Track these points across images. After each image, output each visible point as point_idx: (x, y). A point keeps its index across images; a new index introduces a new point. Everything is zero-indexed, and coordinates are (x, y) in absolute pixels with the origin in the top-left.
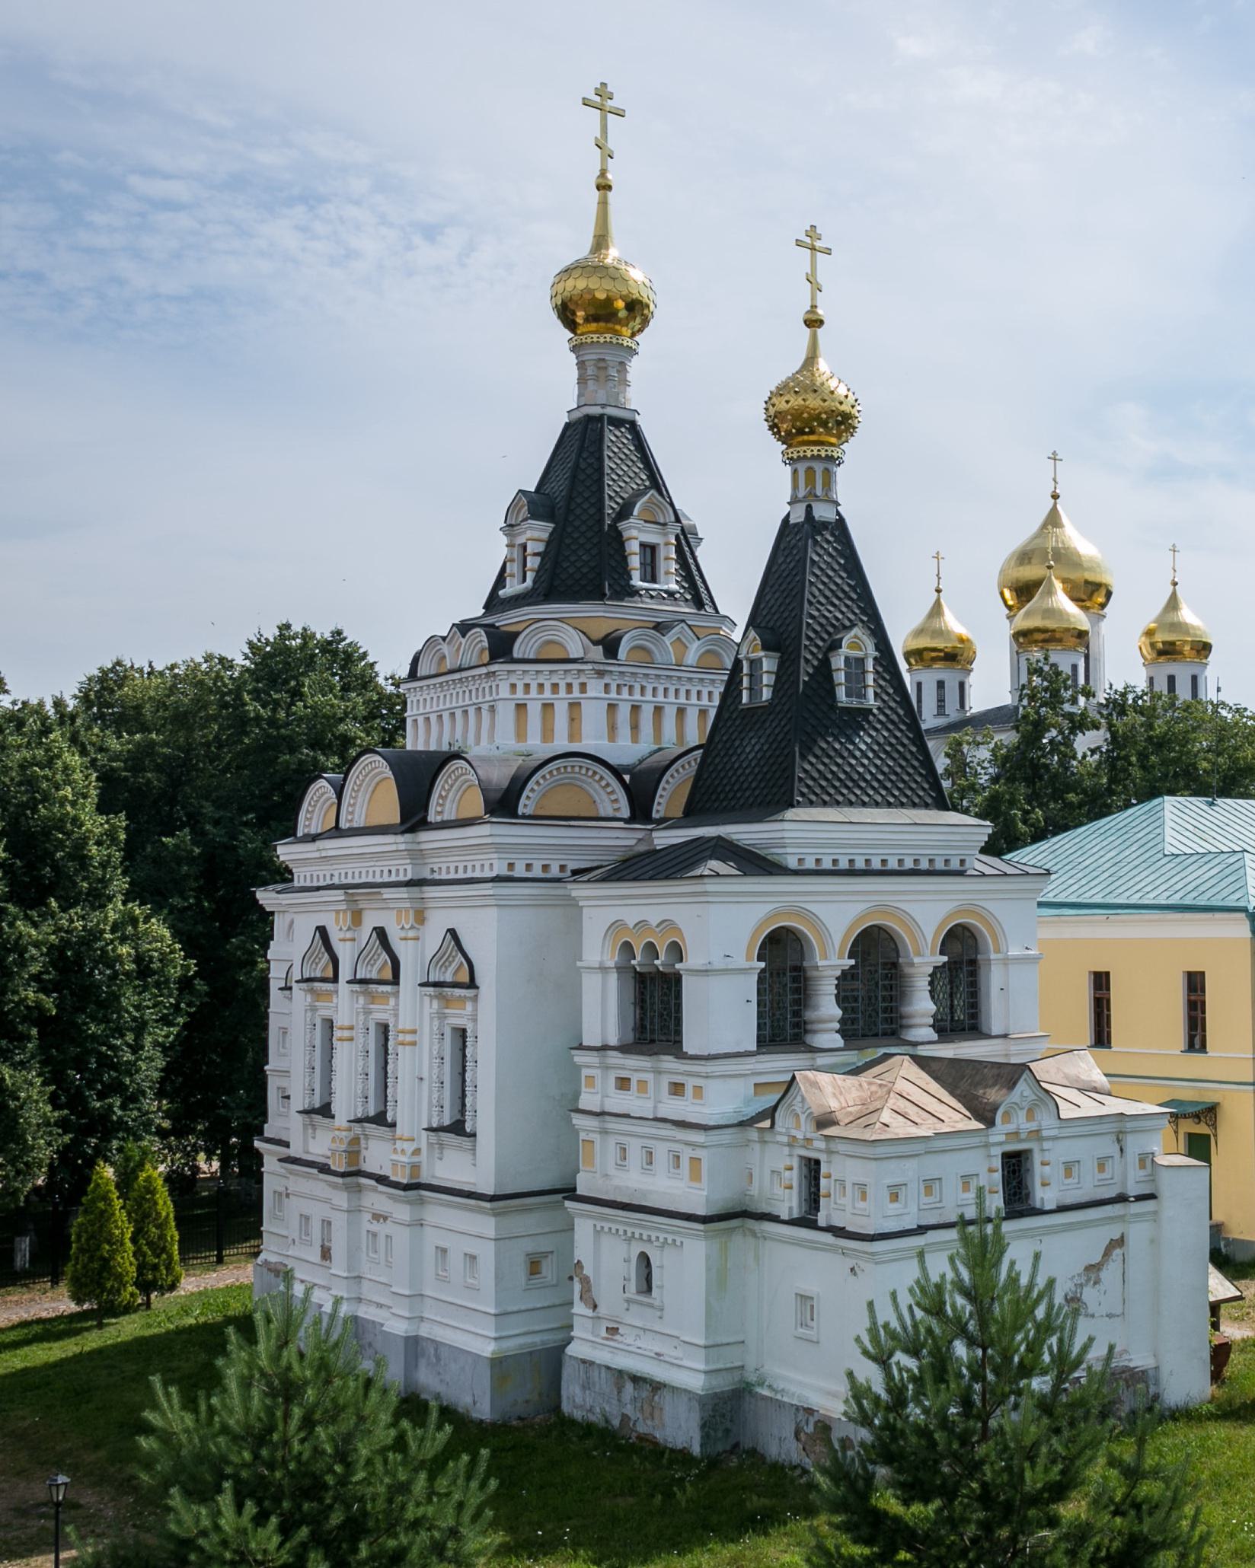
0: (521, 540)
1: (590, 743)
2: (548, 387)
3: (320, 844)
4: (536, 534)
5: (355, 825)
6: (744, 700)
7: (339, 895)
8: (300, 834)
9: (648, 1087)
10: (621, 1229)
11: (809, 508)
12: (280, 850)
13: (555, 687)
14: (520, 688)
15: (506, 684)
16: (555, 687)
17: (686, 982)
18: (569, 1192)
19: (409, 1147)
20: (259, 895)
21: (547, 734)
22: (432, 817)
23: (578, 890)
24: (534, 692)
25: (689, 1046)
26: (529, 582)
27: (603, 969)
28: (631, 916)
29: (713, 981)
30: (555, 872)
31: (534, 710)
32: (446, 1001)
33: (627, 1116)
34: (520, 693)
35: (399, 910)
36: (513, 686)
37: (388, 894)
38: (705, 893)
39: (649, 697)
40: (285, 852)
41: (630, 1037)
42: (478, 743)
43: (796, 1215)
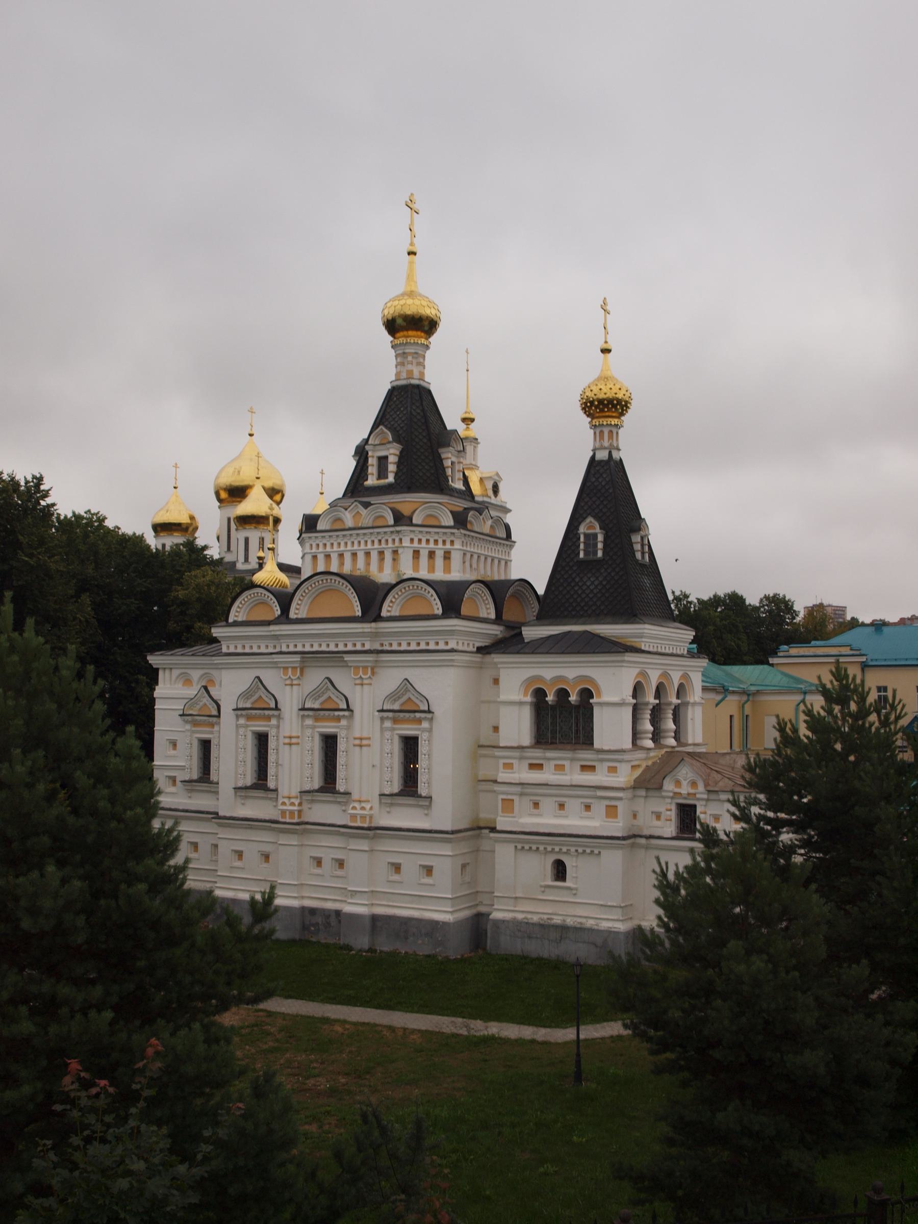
0: (382, 453)
1: (423, 573)
2: (378, 369)
3: (272, 628)
4: (392, 451)
5: (299, 616)
6: (582, 555)
7: (297, 658)
8: (231, 620)
9: (562, 769)
10: (573, 849)
11: (610, 453)
12: (213, 630)
13: (436, 542)
14: (416, 540)
15: (408, 539)
16: (436, 542)
17: (596, 711)
18: (493, 830)
19: (368, 806)
20: (149, 658)
21: (432, 569)
22: (384, 613)
23: (497, 658)
24: (424, 544)
25: (597, 744)
26: (391, 479)
27: (521, 703)
28: (571, 673)
29: (605, 709)
30: (471, 649)
31: (424, 554)
32: (395, 721)
33: (547, 785)
34: (416, 544)
35: (357, 668)
36: (412, 540)
37: (347, 658)
38: (623, 661)
39: (321, 549)
40: (216, 632)
41: (533, 742)
42: (381, 569)
43: (674, 834)
